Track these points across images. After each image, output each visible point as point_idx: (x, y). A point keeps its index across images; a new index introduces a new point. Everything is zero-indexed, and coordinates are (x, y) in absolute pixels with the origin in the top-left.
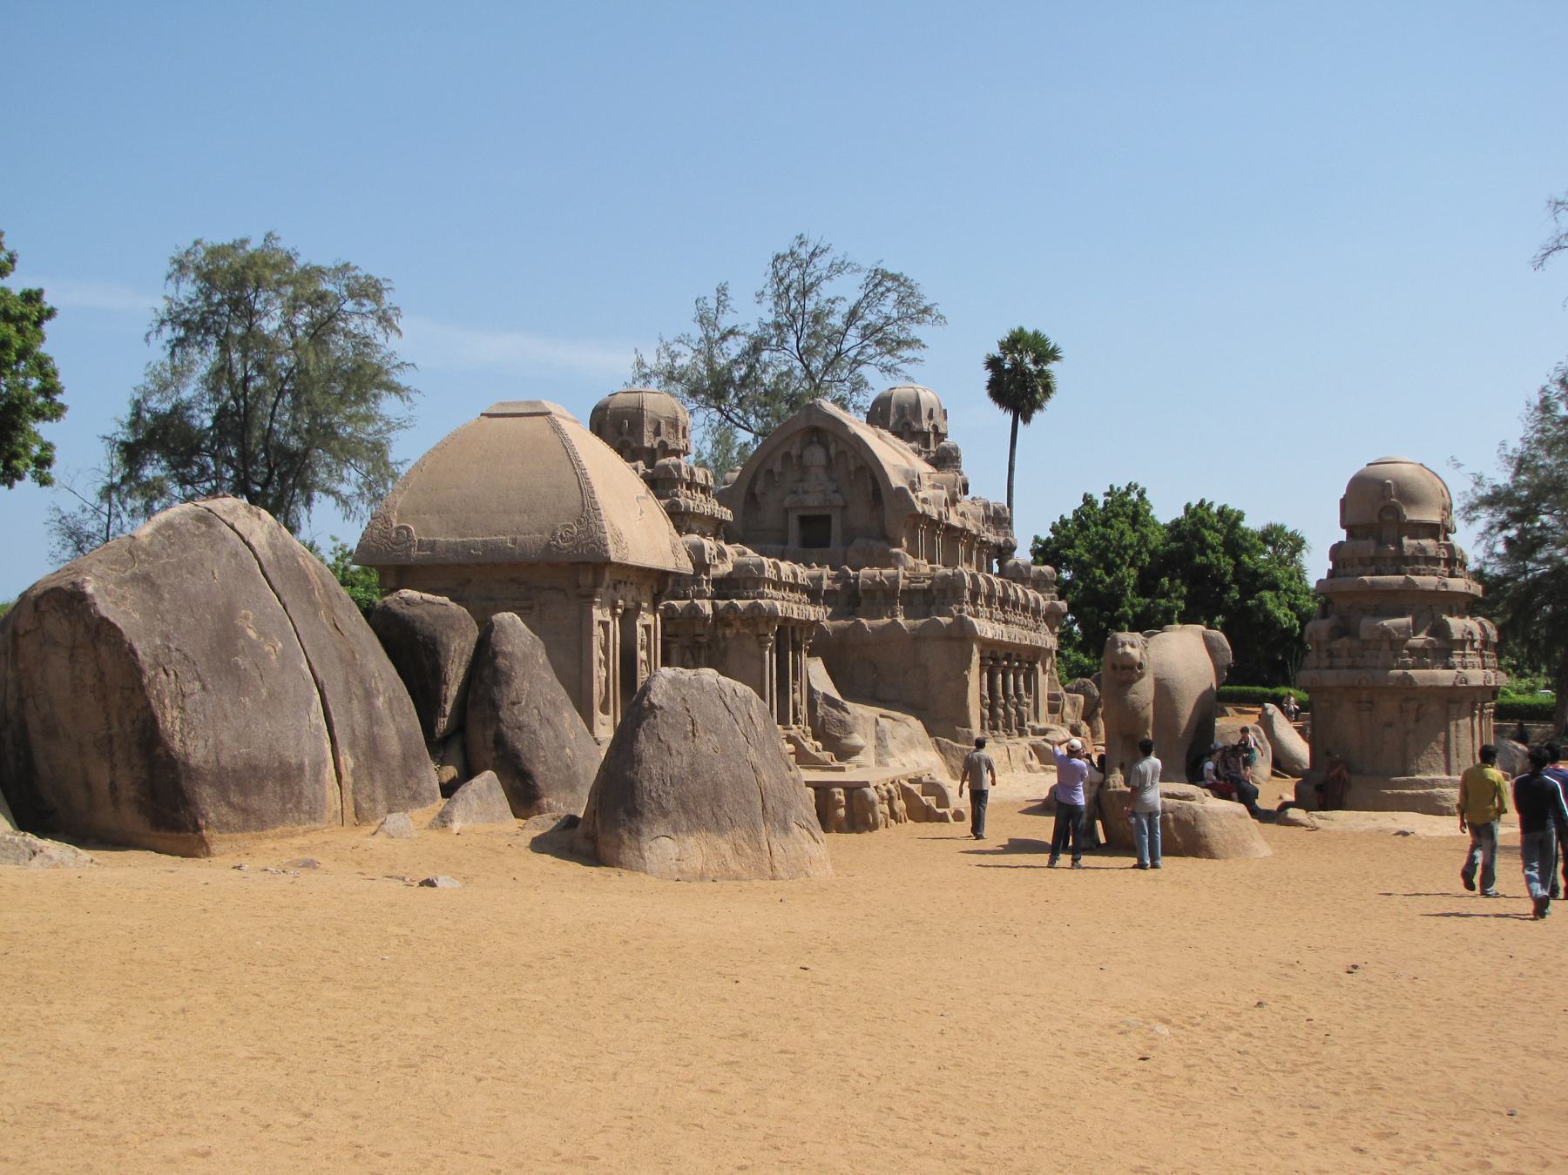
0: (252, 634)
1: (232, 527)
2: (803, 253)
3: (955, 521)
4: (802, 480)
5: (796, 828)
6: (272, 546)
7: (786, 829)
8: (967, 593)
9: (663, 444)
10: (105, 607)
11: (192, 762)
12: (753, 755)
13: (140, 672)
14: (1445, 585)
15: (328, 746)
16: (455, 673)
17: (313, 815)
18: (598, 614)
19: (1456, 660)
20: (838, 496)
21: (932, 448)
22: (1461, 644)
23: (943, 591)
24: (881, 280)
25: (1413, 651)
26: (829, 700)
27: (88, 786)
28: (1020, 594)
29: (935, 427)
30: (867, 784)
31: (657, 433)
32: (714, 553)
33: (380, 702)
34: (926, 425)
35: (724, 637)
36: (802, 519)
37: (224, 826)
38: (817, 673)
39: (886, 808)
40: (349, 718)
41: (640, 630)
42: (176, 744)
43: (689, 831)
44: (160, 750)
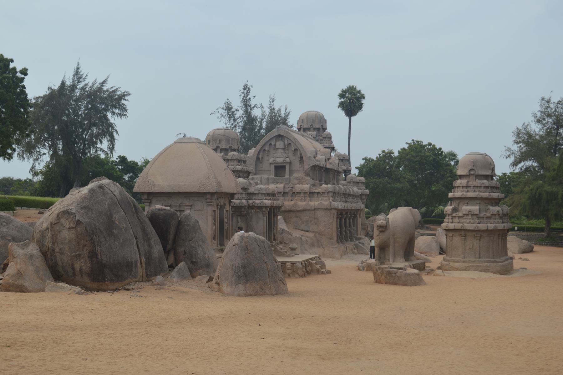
0: (117, 222)
3: (329, 166)
5: (278, 281)
6: (120, 194)
7: (276, 281)
12: (265, 259)
16: (172, 231)
20: (288, 159)
27: (73, 269)
33: (152, 241)
35: (251, 212)
36: (276, 167)
37: (112, 281)
41: (225, 212)
42: (99, 257)
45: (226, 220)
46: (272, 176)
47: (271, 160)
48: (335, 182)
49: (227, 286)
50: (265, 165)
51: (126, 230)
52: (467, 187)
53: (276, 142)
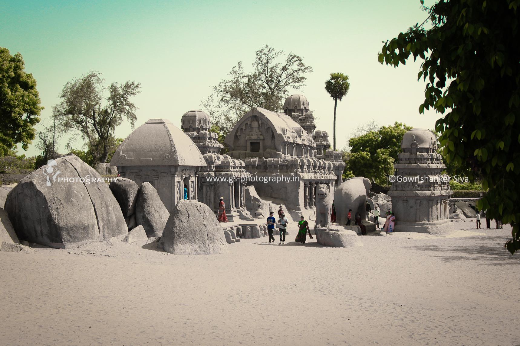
1: (71, 164)
2: (266, 50)
3: (299, 142)
4: (251, 131)
5: (217, 241)
6: (82, 168)
7: (214, 242)
8: (299, 166)
9: (202, 127)
10: (38, 187)
11: (60, 226)
12: (205, 222)
13: (47, 203)
14: (429, 166)
15: (96, 220)
16: (132, 199)
17: (92, 238)
18: (177, 179)
19: (432, 188)
21: (304, 114)
22: (434, 183)
23: (291, 165)
24: (292, 58)
25: (419, 186)
26: (255, 199)
27: (36, 231)
28: (322, 163)
29: (305, 107)
30: (257, 225)
31: (200, 123)
32: (216, 158)
33: (110, 208)
34: (302, 107)
36: (252, 143)
38: (252, 191)
39: (263, 232)
40: (102, 212)
41: (190, 183)
42: (56, 221)
43: (186, 243)
44: (52, 223)
45: (191, 189)
46: (248, 151)
47: (247, 138)
48: (308, 156)
49: (169, 246)
50: (242, 142)
51: (84, 198)
52: (409, 159)
53: (252, 121)
